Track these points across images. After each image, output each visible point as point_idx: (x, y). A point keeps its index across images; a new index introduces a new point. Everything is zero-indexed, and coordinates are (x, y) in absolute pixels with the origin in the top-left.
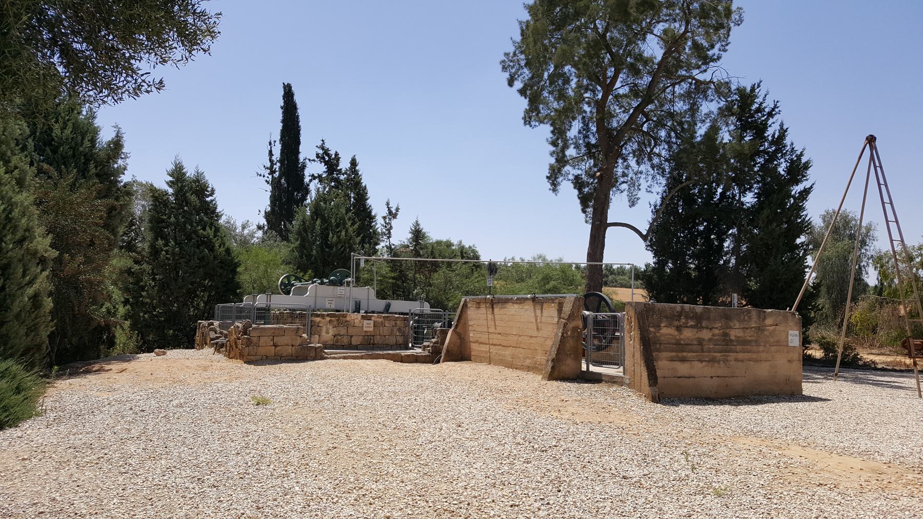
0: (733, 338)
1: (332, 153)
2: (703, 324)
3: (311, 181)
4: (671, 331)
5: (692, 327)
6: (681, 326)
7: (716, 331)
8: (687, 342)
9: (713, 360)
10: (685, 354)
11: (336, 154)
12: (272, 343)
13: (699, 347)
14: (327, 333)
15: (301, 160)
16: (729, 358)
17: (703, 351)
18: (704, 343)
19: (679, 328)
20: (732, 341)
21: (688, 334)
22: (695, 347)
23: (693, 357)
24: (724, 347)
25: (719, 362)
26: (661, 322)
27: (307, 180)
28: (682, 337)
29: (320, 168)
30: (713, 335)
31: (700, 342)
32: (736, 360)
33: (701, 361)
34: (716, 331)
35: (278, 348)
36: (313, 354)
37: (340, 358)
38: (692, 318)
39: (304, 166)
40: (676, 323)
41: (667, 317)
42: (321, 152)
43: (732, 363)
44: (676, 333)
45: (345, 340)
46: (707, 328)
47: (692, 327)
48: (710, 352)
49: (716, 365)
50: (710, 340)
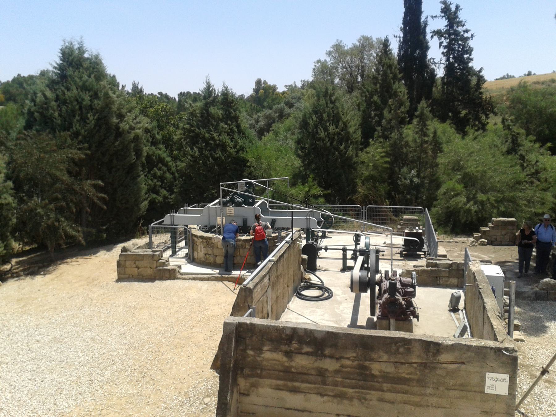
0: (375, 372)
1: (453, 8)
2: (327, 352)
3: (432, 37)
4: (279, 356)
5: (307, 353)
6: (291, 352)
7: (348, 363)
8: (300, 370)
9: (341, 396)
10: (297, 384)
11: (457, 7)
12: (134, 266)
13: (319, 379)
14: (201, 251)
15: (423, 18)
16: (368, 397)
17: (324, 383)
18: (327, 374)
19: (288, 354)
20: (374, 376)
21: (301, 362)
22: (312, 378)
23: (310, 389)
24: (360, 383)
25: (351, 399)
26: (263, 345)
27: (428, 37)
28: (293, 364)
29: (442, 24)
30: (342, 366)
31: (321, 373)
32: (381, 400)
33: (322, 395)
34: (348, 363)
35: (140, 270)
36: (167, 275)
37: (190, 279)
38: (308, 344)
39: (426, 25)
40: (285, 348)
41: (271, 340)
42: (443, 6)
43: (374, 403)
44: (285, 359)
45: (211, 259)
46: (331, 357)
47: (307, 353)
48: (336, 384)
49: (346, 402)
50: (337, 372)
